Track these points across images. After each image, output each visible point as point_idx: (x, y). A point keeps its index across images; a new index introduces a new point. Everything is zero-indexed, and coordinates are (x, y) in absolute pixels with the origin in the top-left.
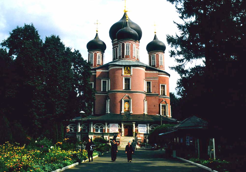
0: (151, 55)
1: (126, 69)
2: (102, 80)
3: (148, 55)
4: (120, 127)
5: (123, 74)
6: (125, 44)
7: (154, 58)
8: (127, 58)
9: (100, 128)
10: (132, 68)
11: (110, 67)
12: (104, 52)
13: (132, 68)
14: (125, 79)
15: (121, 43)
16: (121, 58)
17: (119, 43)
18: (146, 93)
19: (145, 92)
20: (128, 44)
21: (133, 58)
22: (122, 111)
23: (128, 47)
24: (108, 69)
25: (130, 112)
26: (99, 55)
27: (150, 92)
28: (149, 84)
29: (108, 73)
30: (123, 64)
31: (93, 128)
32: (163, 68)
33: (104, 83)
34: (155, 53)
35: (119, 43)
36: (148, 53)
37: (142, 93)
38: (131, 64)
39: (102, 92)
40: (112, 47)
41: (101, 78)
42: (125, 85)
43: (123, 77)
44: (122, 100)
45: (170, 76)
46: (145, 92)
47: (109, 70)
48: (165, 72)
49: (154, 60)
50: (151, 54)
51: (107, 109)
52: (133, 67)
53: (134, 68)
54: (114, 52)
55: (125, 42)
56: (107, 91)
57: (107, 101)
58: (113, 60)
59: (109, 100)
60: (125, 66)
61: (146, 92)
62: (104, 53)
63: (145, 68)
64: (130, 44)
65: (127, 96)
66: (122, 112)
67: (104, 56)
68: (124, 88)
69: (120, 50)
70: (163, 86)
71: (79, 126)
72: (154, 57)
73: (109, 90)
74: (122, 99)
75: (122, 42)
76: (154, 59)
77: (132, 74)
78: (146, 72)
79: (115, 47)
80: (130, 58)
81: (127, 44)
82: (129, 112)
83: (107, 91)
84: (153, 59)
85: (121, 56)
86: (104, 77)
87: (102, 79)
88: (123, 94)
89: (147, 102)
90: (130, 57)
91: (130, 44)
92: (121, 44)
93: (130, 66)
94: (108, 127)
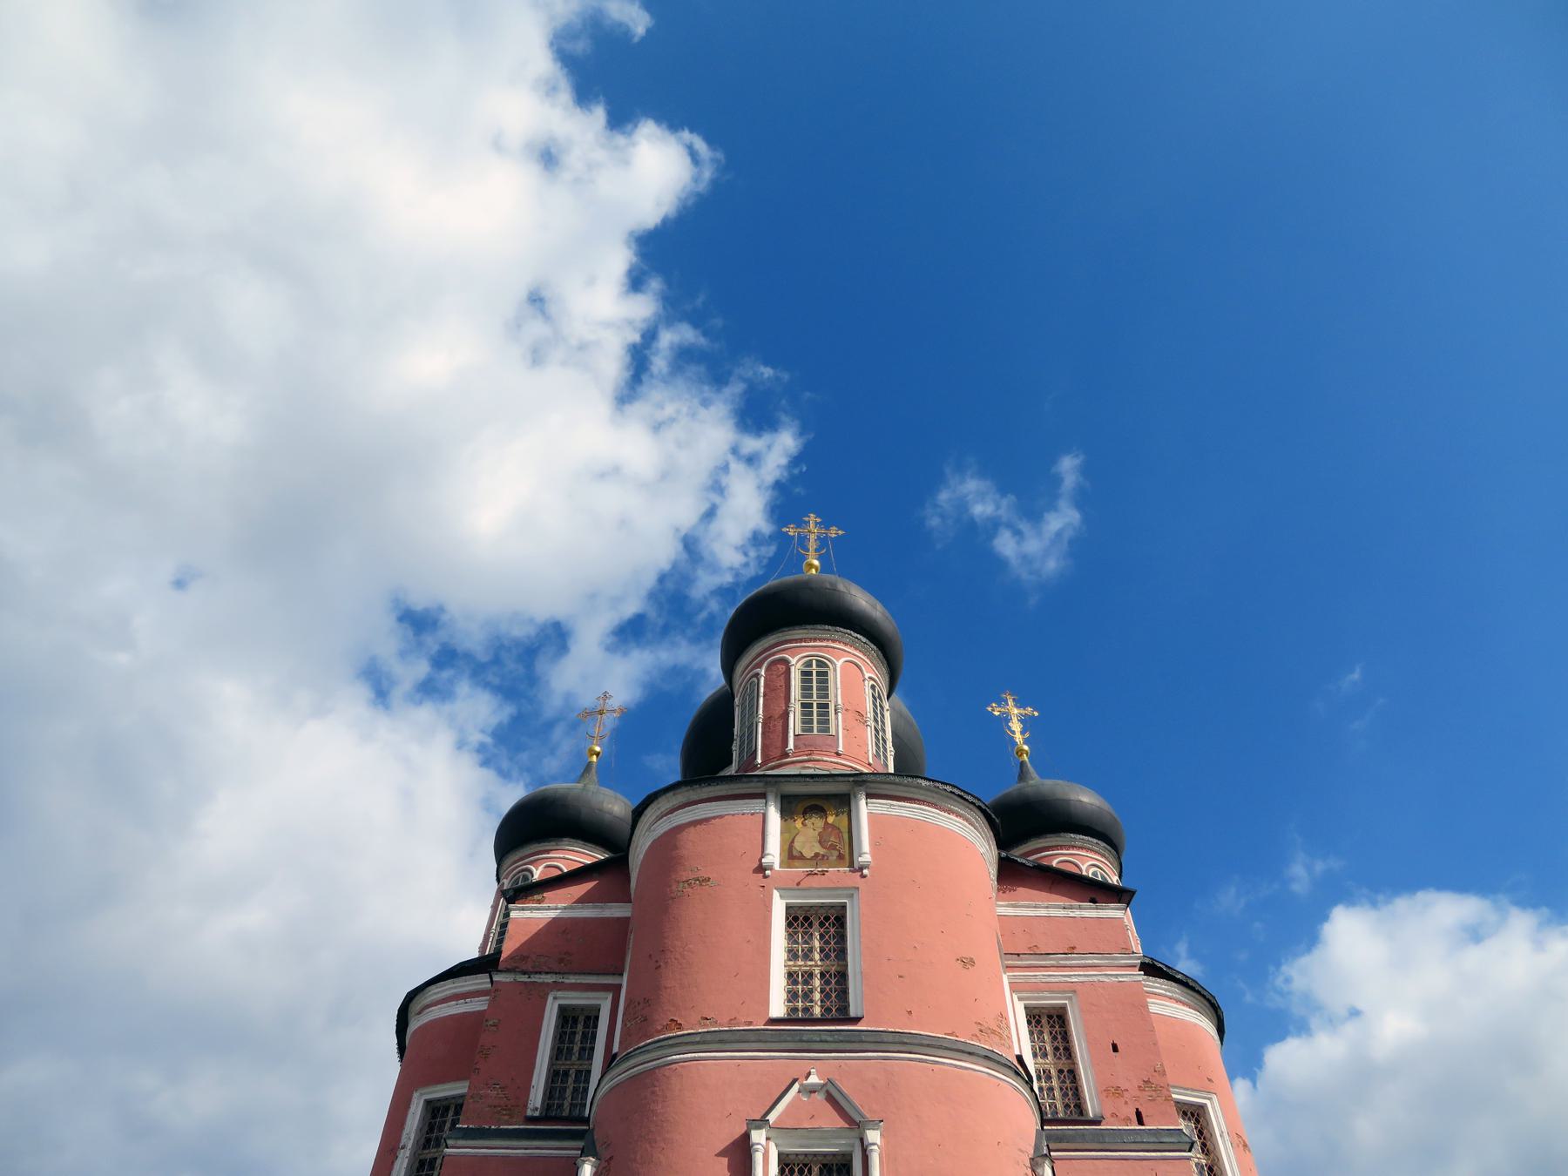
5: (774, 853)
6: (793, 661)
10: (865, 809)
13: (865, 809)
20: (820, 664)
21: (871, 761)
23: (818, 677)
29: (624, 922)
33: (577, 1024)
37: (989, 1058)
43: (776, 894)
53: (882, 807)
77: (866, 858)
78: (1004, 910)
80: (838, 754)
81: (809, 664)
88: (778, 1063)
90: (841, 749)
91: (839, 664)
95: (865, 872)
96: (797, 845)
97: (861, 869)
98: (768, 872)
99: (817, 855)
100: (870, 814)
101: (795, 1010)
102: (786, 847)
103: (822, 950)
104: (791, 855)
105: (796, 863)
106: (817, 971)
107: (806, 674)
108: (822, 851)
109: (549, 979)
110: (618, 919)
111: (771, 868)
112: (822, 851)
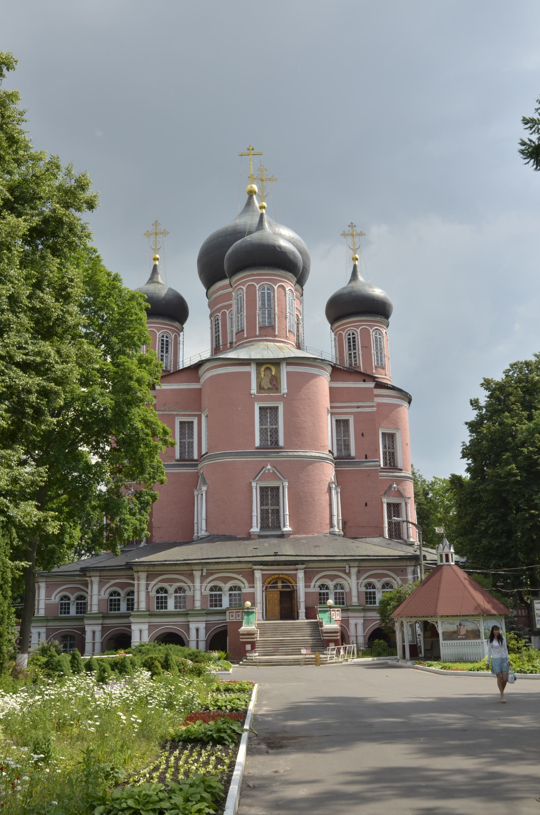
0: (344, 334)
1: (263, 373)
2: (176, 418)
3: (333, 334)
4: (250, 587)
6: (257, 287)
7: (354, 341)
8: (266, 336)
9: (176, 592)
10: (284, 370)
11: (205, 372)
12: (182, 330)
14: (261, 408)
15: (243, 284)
16: (245, 336)
17: (236, 287)
18: (335, 459)
19: (333, 454)
20: (268, 289)
22: (252, 527)
24: (198, 380)
25: (285, 529)
26: (165, 339)
27: (349, 457)
28: (344, 426)
29: (199, 391)
30: (253, 357)
31: (148, 593)
32: (386, 375)
33: (186, 426)
34: (357, 327)
35: (236, 287)
36: (331, 329)
38: (281, 356)
39: (177, 461)
40: (208, 311)
41: (175, 413)
42: (261, 430)
43: (256, 403)
44: (254, 484)
45: (409, 402)
46: (333, 454)
47: (202, 380)
48: (393, 388)
49: (354, 349)
50: (343, 330)
51: (195, 521)
52: (288, 364)
53: (292, 369)
54: (217, 325)
55: (258, 281)
56: (196, 457)
57: (196, 493)
58: (212, 355)
59: (204, 488)
60: (260, 363)
61: (335, 454)
62: (181, 334)
63: (330, 369)
64: (276, 288)
65: (269, 470)
66: (252, 530)
67: (181, 343)
68: (257, 443)
69: (239, 311)
70: (390, 438)
71: (96, 587)
72: (354, 338)
73: (203, 452)
74: (251, 483)
75: (247, 281)
76: (354, 345)
79: (219, 310)
81: (264, 289)
82: (280, 527)
83: (196, 457)
84: (350, 346)
85: (243, 330)
86: (185, 410)
87: (177, 415)
89: (339, 490)
90: (277, 333)
92: (244, 288)
93: (276, 363)
94: (203, 588)
95: (285, 396)
96: (262, 384)
97: (284, 394)
98: (253, 396)
99: (269, 388)
100: (287, 372)
101: (262, 444)
102: (258, 385)
103: (270, 422)
104: (260, 388)
105: (262, 391)
106: (269, 430)
107: (263, 294)
108: (271, 387)
109: (175, 413)
110: (196, 389)
111: (254, 395)
112: (271, 387)
